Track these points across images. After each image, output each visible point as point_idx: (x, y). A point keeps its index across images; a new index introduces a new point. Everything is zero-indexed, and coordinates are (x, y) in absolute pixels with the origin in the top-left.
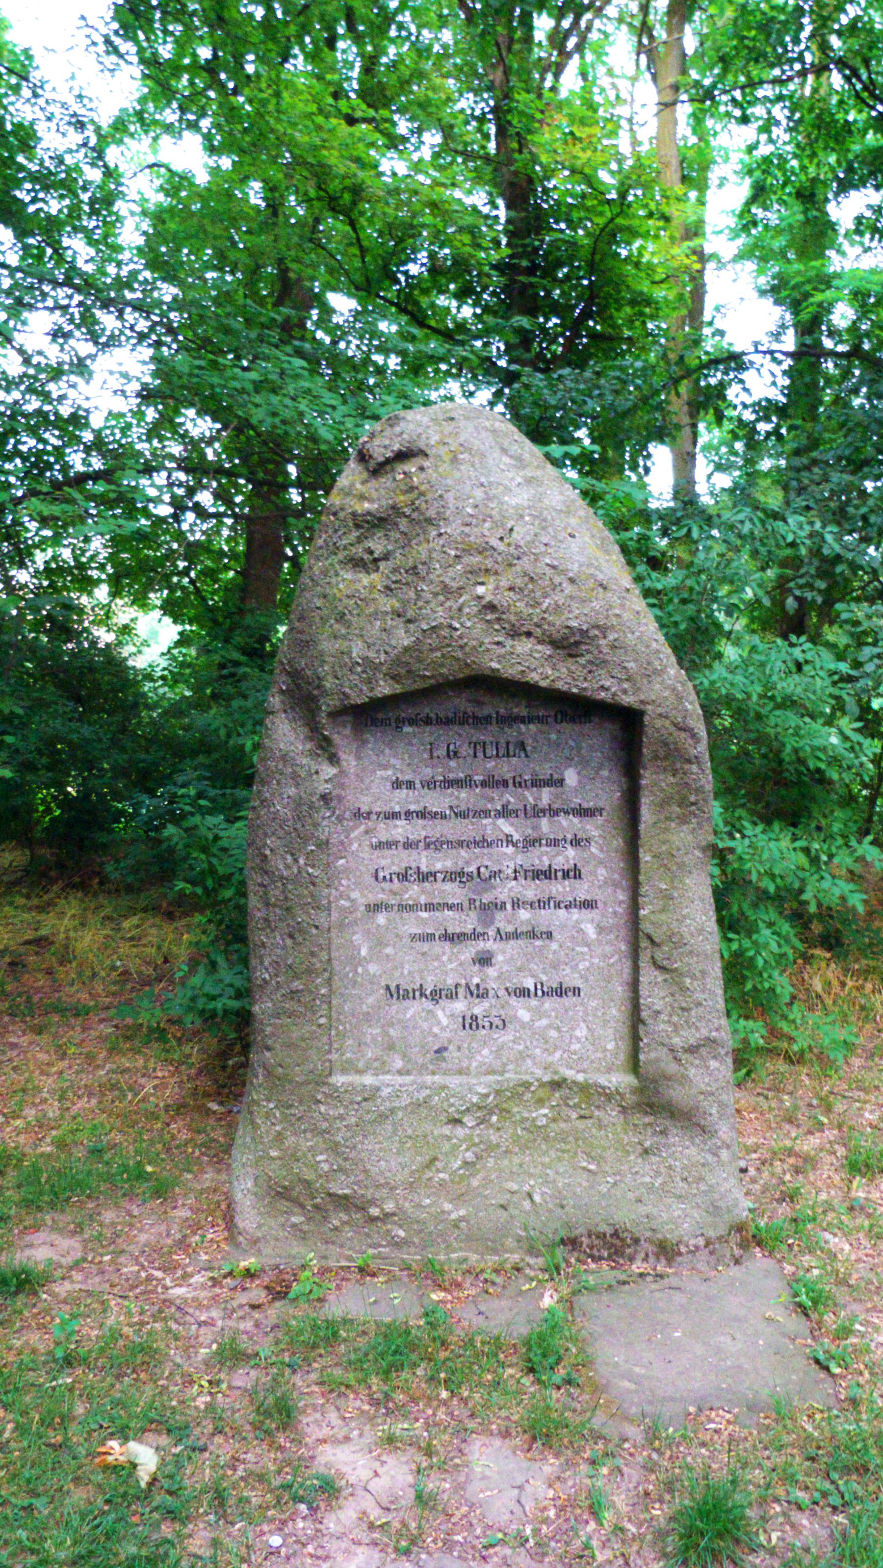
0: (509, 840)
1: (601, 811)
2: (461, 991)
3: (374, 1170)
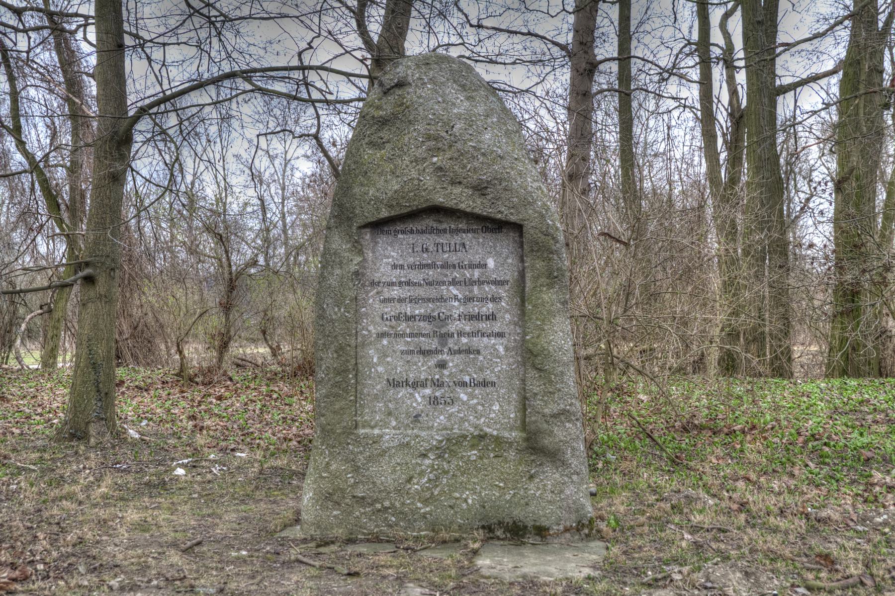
0: (456, 298)
1: (507, 282)
2: (429, 383)
3: (379, 482)
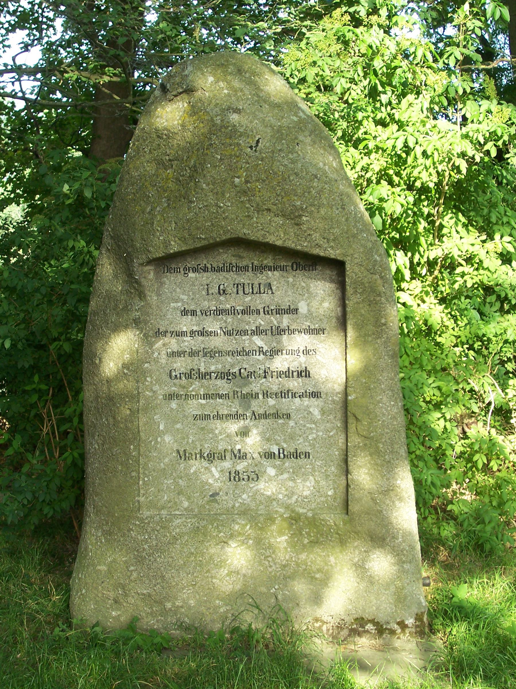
0: (261, 350)
